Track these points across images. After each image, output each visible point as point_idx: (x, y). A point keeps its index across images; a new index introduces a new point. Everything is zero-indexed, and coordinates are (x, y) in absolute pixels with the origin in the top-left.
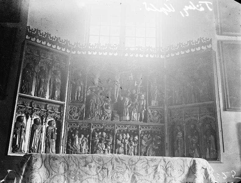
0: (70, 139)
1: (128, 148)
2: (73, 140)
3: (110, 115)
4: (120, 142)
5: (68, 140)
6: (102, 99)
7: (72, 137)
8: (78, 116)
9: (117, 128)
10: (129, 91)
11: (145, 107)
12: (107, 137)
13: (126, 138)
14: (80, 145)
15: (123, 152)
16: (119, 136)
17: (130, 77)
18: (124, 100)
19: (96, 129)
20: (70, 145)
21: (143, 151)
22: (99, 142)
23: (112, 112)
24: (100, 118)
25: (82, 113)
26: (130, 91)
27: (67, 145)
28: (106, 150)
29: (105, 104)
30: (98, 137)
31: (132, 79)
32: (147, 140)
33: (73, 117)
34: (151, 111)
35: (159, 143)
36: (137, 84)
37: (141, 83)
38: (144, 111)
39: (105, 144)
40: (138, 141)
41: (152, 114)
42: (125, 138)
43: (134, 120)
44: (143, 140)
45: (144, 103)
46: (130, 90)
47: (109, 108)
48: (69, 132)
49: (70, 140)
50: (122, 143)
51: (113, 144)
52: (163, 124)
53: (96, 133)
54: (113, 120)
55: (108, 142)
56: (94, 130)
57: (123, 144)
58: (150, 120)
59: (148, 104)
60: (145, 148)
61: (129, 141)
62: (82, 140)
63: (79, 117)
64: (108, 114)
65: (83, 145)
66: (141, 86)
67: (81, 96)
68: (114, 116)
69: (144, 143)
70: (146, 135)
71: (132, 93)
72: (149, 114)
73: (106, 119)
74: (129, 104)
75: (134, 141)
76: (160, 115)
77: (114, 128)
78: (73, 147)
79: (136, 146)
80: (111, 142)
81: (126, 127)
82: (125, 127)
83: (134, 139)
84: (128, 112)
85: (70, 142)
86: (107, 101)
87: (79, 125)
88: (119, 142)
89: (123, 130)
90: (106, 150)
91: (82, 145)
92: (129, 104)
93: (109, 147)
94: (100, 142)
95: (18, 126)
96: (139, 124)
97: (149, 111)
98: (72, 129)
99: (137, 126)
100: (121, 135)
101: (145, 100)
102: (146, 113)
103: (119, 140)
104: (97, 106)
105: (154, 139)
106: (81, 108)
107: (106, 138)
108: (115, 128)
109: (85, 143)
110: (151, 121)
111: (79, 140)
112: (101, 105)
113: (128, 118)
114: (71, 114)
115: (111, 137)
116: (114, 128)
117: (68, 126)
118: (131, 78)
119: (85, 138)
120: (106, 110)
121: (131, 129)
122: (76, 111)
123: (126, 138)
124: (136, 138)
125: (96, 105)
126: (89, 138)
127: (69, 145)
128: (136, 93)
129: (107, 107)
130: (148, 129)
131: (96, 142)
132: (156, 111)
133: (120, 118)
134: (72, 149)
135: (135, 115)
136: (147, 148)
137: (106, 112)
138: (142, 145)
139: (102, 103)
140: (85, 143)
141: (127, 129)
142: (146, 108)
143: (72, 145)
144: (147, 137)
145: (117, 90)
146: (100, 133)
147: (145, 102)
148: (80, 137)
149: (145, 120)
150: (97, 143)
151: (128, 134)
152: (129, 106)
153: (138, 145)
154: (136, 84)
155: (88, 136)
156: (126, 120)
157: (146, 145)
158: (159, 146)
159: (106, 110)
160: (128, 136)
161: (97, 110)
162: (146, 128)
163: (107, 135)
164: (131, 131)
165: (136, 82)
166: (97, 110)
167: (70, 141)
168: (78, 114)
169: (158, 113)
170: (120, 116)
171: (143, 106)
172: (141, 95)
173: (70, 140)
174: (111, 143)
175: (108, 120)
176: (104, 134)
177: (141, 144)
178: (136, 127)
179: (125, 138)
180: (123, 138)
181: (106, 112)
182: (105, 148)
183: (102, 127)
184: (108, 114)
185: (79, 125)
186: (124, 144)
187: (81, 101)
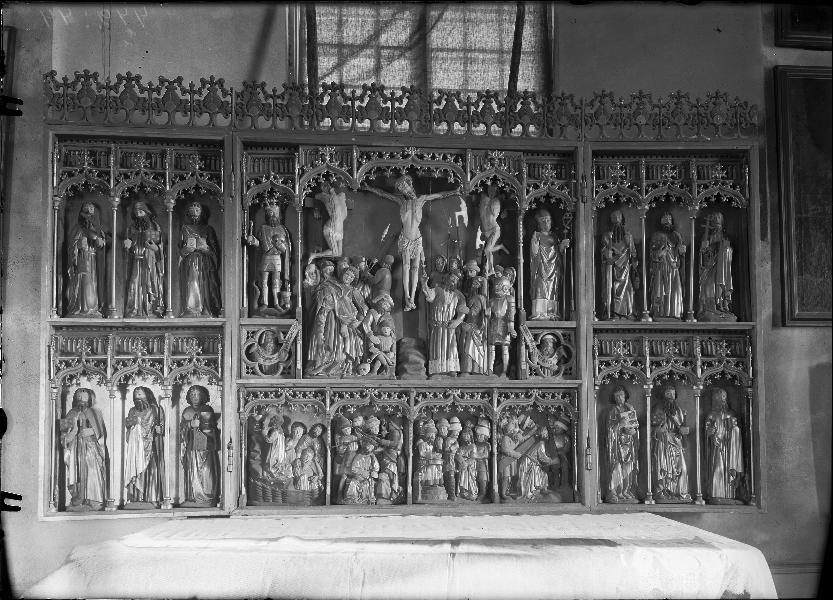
0: (254, 445)
1: (457, 467)
2: (266, 447)
3: (392, 355)
4: (432, 447)
5: (249, 449)
6: (361, 301)
7: (264, 438)
8: (278, 364)
9: (416, 402)
10: (455, 266)
11: (512, 324)
12: (385, 432)
13: (450, 433)
14: (294, 465)
16: (427, 431)
17: (457, 214)
18: (440, 299)
19: (344, 409)
20: (256, 466)
21: (508, 474)
22: (358, 452)
23: (399, 343)
24: (356, 370)
25: (292, 354)
26: (460, 267)
27: (248, 464)
28: (384, 477)
29: (371, 317)
30: (353, 432)
31: (466, 221)
32: (521, 438)
33: (260, 366)
34: (536, 337)
35: (558, 444)
36: (482, 238)
37: (497, 235)
38: (508, 337)
39: (380, 457)
40: (490, 440)
41: (538, 346)
42: (445, 432)
43: (476, 371)
44: (507, 439)
45: (508, 311)
46: (459, 262)
47: (388, 330)
48: (251, 419)
49: (257, 448)
50: (435, 449)
51: (405, 454)
52: (570, 383)
53: (348, 421)
54: (405, 375)
55: (388, 448)
56: (337, 411)
58: (530, 369)
59: (523, 312)
60: (514, 464)
61: (461, 441)
62: (300, 442)
63: (284, 368)
64: (385, 352)
65: (302, 465)
66: (499, 248)
67: (283, 288)
68: (406, 360)
69: (510, 446)
70: (516, 421)
71: (465, 273)
72: (527, 347)
73: (379, 372)
74: (455, 318)
75: (478, 444)
76: (567, 349)
77: (408, 402)
78: (270, 473)
79: (484, 459)
80: (399, 447)
81: (449, 395)
82: (446, 396)
84: (456, 344)
85: (258, 457)
86: (377, 307)
87: (284, 396)
88: (426, 448)
90: (384, 477)
91: (299, 464)
92: (455, 318)
93: (393, 468)
94: (362, 450)
95: (66, 425)
96: (494, 386)
97: (528, 338)
98: (260, 409)
99: (488, 393)
100: (432, 424)
101: (513, 300)
102: (515, 344)
103: (427, 439)
104: (345, 329)
105: (545, 433)
106: (285, 333)
107: (380, 436)
108: (412, 402)
109: (310, 455)
110: (534, 372)
111: (286, 446)
112: (357, 324)
113: (454, 365)
114: (250, 356)
115: (397, 434)
116: (408, 402)
117: (246, 402)
118: (461, 217)
119: (309, 439)
120: (375, 339)
121: (467, 401)
122: (271, 345)
123: (450, 433)
124: (484, 431)
125: (339, 323)
126: (321, 439)
127: (254, 466)
128: (481, 273)
129: (378, 327)
130: (523, 402)
131: (347, 452)
132: (550, 337)
133: (427, 365)
134: (264, 481)
135: (478, 353)
136: (520, 461)
137: (376, 346)
138: (505, 454)
139: (360, 311)
140: (310, 455)
141: (453, 403)
142: (517, 328)
143: (265, 465)
144: (521, 426)
145: (412, 261)
146: (360, 421)
147: (513, 305)
148: (288, 436)
149: (514, 371)
150: (351, 457)
151: (456, 420)
152: (457, 323)
153: (491, 454)
154: (479, 242)
155: (319, 431)
156: (450, 374)
158: (559, 457)
159: (375, 339)
160: (458, 427)
161: (344, 339)
162: (517, 396)
163: (383, 428)
164: (466, 408)
165: (479, 233)
166: (344, 339)
167: (258, 452)
168: (276, 355)
169: (557, 345)
170: (427, 358)
171: (506, 319)
172: (499, 279)
173: (257, 448)
174: (399, 452)
175: (387, 375)
176: (375, 425)
177: (501, 452)
178: (482, 397)
179: (445, 432)
180: (438, 435)
181: (376, 346)
182: (379, 473)
183: (367, 401)
184: (385, 352)
185: (284, 396)
186: (445, 455)
187: (284, 307)
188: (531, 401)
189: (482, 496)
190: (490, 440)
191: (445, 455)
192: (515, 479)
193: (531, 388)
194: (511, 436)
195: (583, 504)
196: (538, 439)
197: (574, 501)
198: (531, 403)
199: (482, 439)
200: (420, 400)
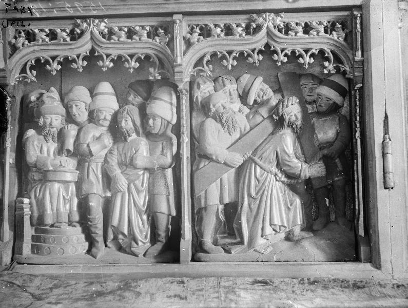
13: (93, 117)
15: (76, 217)
42: (82, 115)
50: (60, 151)
57: (71, 163)
60: (229, 176)
61: (116, 131)
75: (148, 134)
79: (163, 168)
81: (83, 33)
82: (74, 36)
83: (144, 115)
89: (67, 62)
103: (39, 130)
105: (293, 110)
123: (93, 117)
136: (241, 171)
138: (208, 157)
144: (243, 97)
153: (177, 158)
157: (238, 160)
158: (327, 159)
160: (108, 101)
162: (228, 31)
177: (199, 154)
186: (82, 157)
188: (260, 40)
189: (159, 247)
190: (177, 129)
191: (82, 157)
192: (232, 211)
193: (260, 12)
194: (218, 118)
195: (378, 266)
196: (279, 122)
197: (357, 259)
198: (260, 46)
199: (156, 126)
200: (20, 45)
